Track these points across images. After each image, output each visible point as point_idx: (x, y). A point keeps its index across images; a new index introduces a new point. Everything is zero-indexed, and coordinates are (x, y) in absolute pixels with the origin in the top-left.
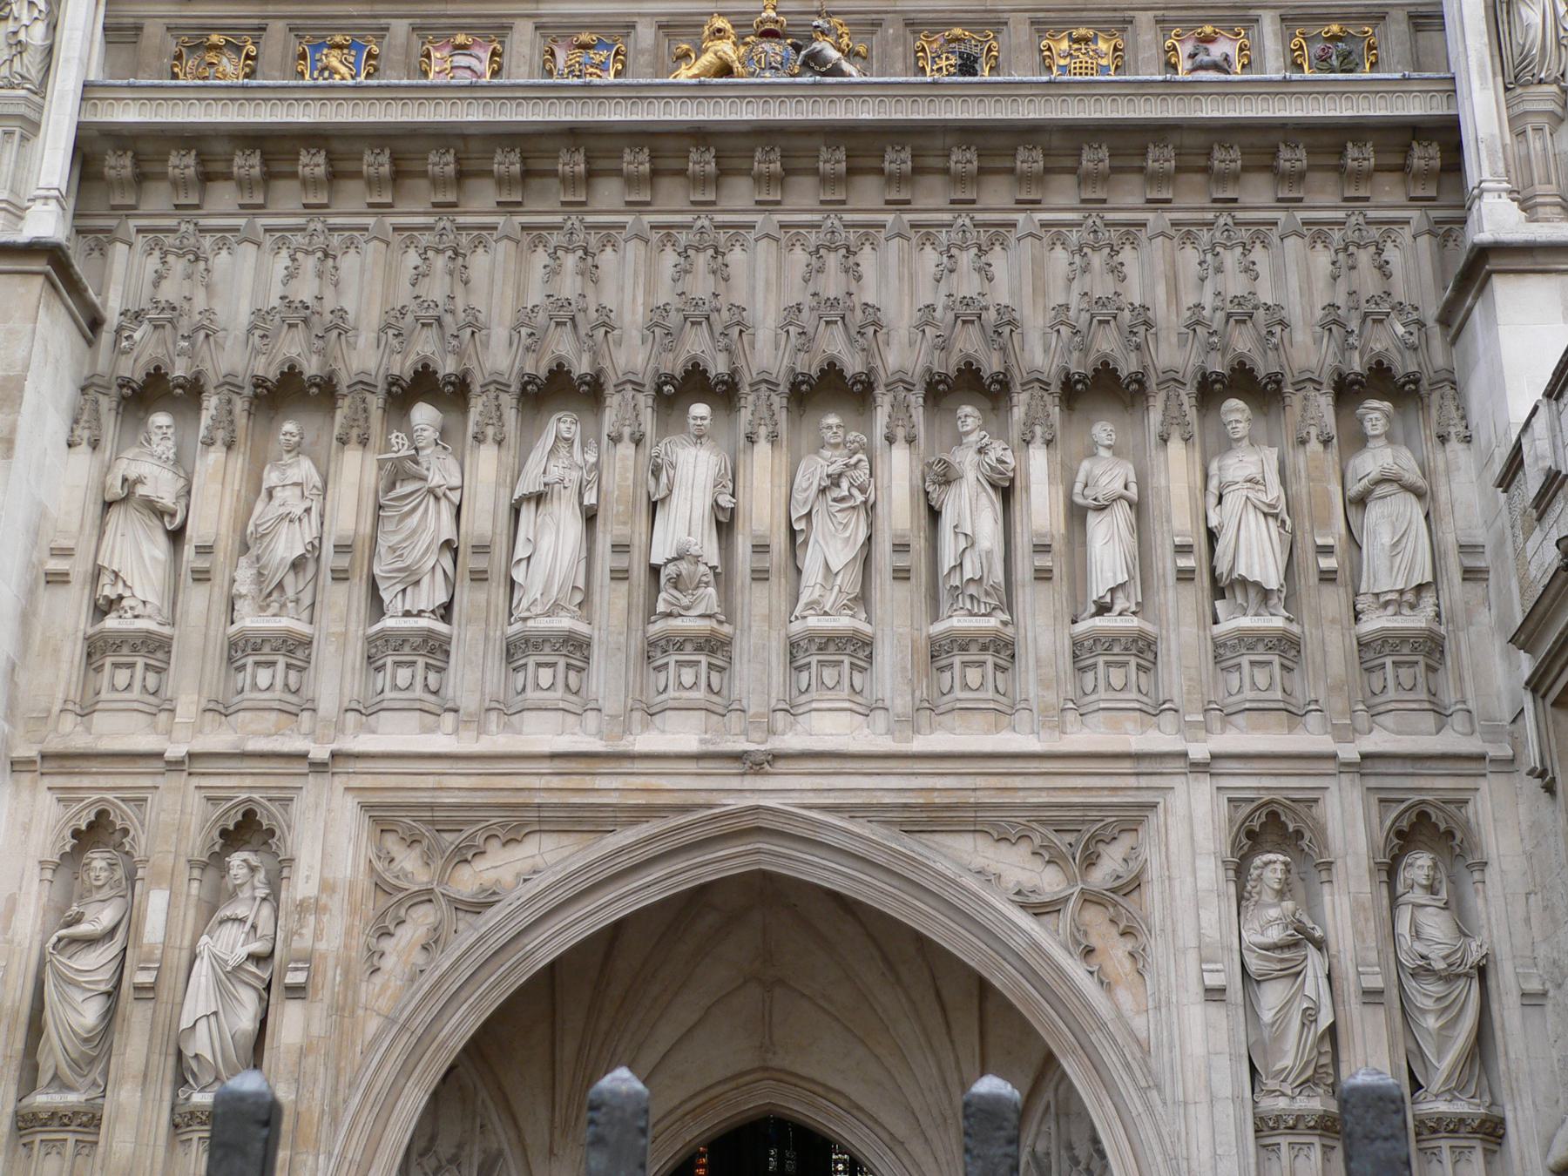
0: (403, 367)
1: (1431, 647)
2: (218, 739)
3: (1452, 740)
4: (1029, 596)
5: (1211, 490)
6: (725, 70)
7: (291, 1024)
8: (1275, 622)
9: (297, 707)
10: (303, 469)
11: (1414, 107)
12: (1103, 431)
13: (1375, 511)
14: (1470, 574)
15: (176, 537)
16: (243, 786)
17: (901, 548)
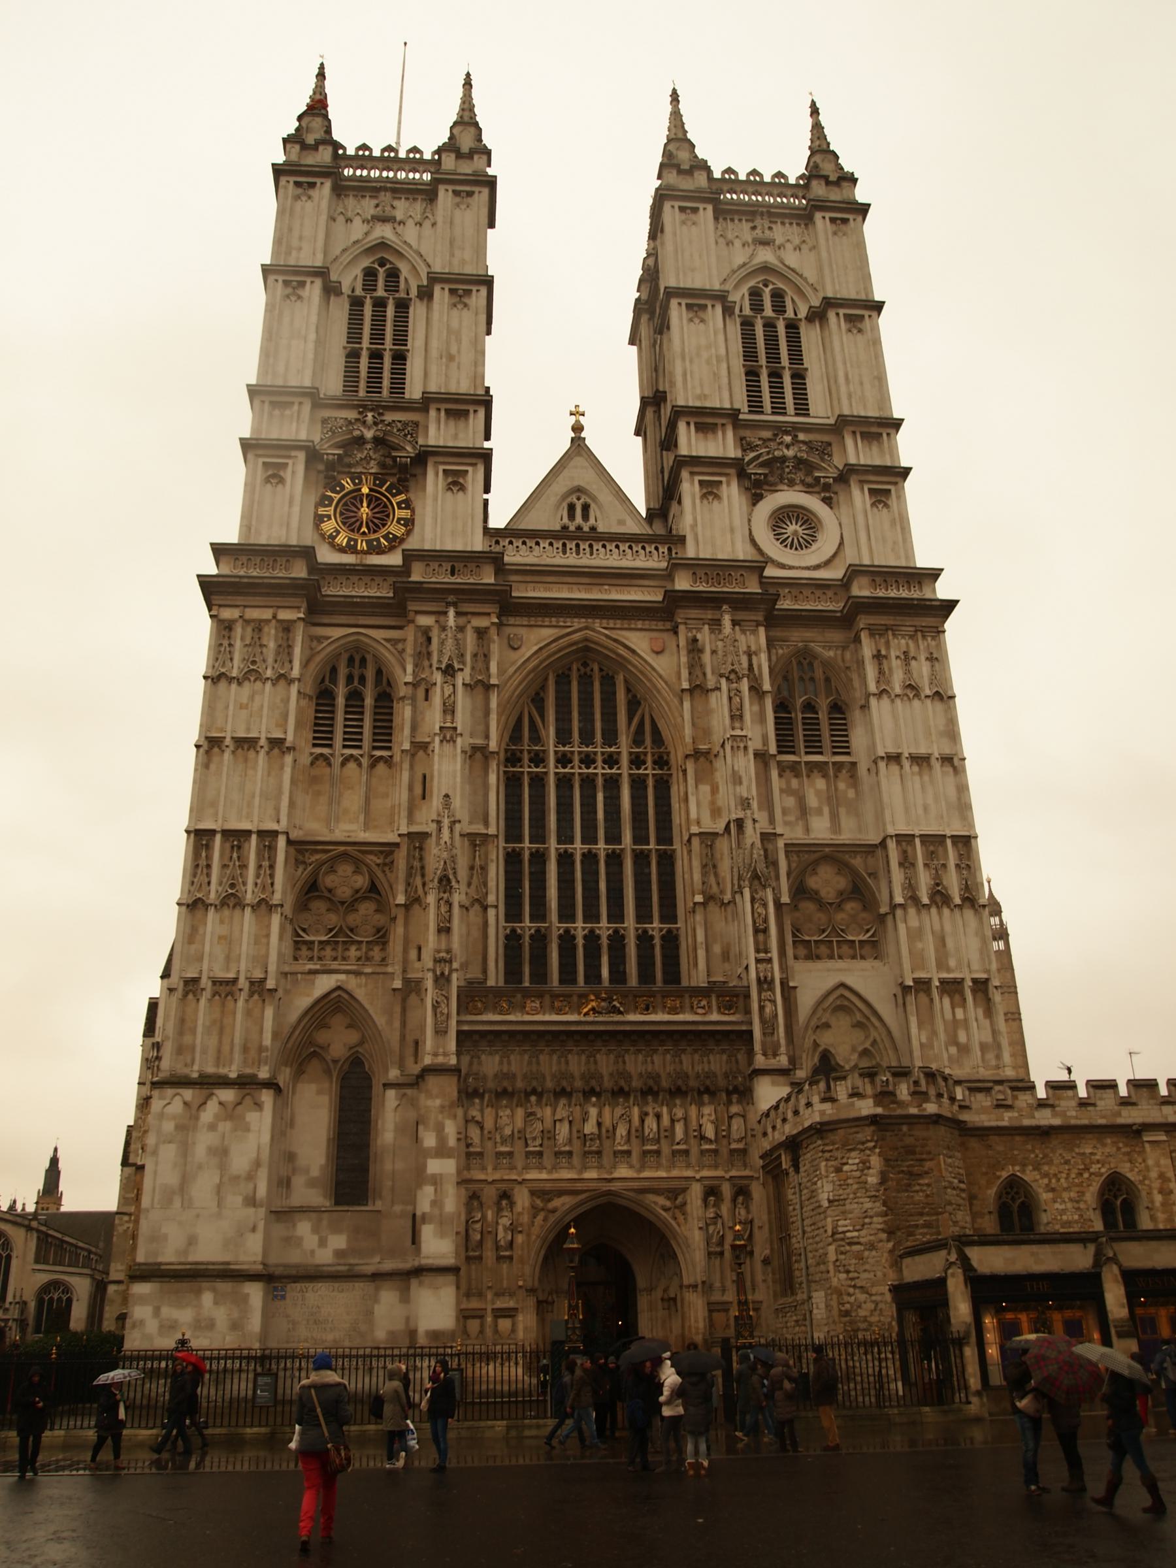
0: (529, 1089)
1: (744, 1152)
2: (497, 1176)
3: (747, 1173)
4: (663, 1141)
5: (700, 1115)
6: (593, 1009)
7: (520, 1239)
8: (713, 1147)
9: (512, 1168)
10: (508, 1112)
11: (744, 1028)
12: (678, 1102)
13: (734, 1121)
14: (753, 1136)
15: (482, 1128)
16: (503, 1186)
17: (637, 1131)
